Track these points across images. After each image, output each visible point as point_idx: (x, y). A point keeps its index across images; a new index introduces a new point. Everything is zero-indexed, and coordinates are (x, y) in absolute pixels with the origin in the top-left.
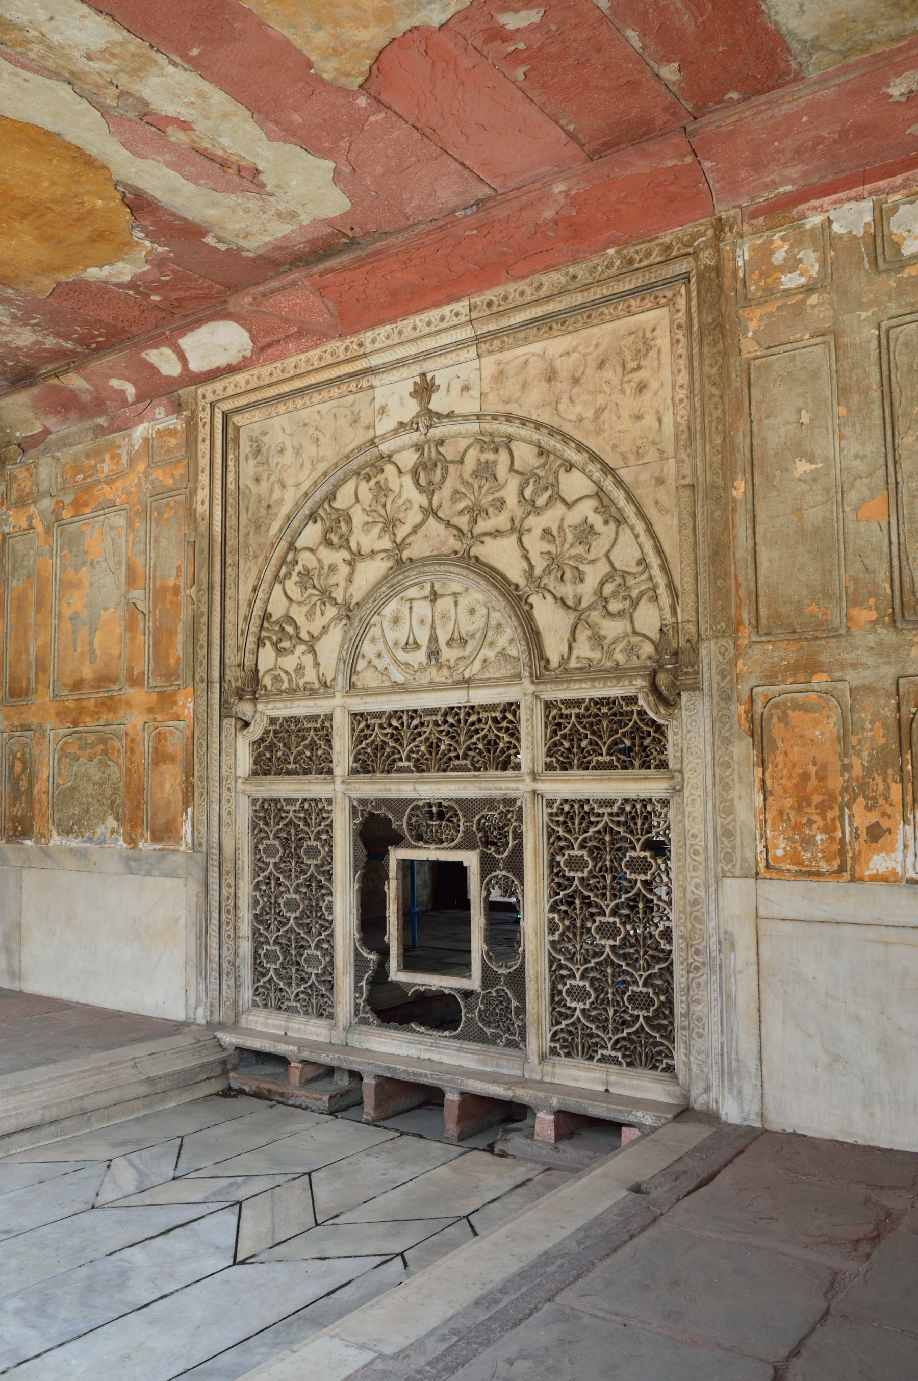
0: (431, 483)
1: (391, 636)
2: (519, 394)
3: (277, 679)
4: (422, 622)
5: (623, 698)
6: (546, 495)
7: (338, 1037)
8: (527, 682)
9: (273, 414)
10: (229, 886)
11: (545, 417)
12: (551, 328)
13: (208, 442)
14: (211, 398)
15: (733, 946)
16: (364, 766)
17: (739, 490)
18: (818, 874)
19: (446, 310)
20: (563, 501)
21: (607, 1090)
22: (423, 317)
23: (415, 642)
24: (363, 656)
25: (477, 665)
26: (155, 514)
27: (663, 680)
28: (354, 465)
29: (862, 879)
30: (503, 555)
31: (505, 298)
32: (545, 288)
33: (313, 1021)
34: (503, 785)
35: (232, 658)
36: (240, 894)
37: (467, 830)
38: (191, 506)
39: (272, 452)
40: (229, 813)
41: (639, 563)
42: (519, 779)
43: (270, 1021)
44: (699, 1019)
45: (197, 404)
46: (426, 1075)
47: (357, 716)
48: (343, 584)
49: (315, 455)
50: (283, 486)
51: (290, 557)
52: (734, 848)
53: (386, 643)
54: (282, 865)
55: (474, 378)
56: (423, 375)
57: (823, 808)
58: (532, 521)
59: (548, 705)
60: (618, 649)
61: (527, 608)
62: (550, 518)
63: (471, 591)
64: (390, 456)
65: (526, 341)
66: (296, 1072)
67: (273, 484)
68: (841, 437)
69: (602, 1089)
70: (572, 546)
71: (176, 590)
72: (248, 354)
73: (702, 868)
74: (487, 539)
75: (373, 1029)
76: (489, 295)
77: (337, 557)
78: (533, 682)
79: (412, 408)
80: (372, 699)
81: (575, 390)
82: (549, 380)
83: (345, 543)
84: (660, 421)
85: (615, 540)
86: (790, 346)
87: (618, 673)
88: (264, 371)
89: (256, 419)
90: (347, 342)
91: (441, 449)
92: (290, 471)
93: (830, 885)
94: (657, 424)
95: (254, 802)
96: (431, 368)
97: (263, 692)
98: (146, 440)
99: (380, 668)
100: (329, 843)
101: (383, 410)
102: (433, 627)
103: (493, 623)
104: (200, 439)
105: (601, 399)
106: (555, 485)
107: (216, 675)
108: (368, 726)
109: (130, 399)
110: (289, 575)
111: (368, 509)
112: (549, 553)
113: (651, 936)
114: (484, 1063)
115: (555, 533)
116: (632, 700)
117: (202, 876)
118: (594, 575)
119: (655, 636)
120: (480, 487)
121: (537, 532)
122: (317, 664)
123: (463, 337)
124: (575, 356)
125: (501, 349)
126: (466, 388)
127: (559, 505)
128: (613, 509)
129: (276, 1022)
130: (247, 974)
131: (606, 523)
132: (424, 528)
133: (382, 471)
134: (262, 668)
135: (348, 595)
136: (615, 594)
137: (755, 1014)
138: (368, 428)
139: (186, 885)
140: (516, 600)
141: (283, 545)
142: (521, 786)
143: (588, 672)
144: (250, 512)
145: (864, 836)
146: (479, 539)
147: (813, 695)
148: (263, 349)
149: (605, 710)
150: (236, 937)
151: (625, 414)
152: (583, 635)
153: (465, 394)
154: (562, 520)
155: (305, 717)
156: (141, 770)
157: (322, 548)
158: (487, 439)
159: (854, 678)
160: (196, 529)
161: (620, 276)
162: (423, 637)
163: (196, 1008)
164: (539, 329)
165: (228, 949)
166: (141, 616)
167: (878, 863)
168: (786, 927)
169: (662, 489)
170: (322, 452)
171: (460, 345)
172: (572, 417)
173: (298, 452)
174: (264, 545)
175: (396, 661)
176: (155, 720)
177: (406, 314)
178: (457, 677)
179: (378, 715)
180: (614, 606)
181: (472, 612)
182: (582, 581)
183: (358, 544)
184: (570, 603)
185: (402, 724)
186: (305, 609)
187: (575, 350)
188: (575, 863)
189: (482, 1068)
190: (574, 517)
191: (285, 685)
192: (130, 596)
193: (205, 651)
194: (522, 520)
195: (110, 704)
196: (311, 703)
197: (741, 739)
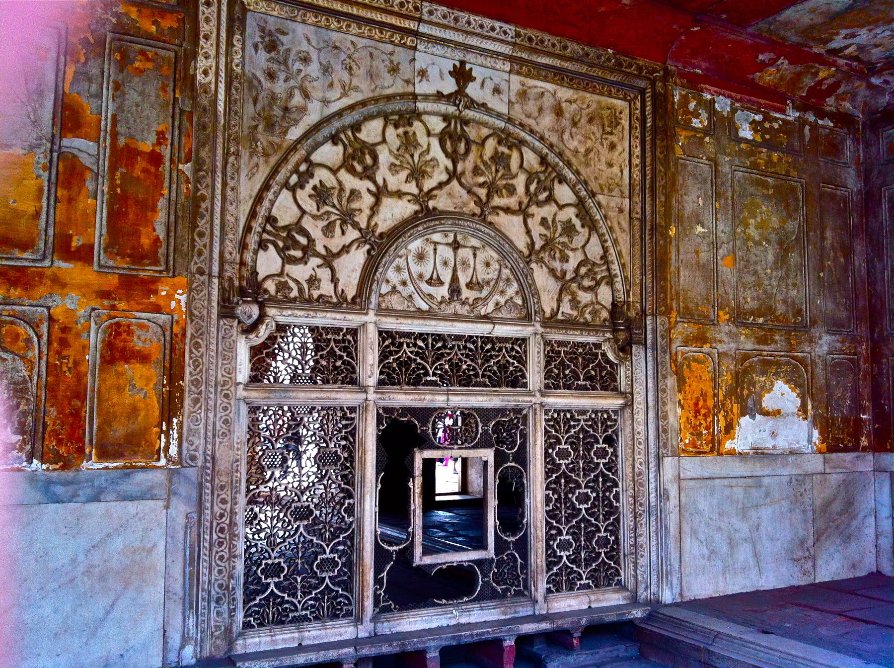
1: (415, 269)
2: (537, 114)
3: (282, 287)
5: (593, 344)
7: (364, 631)
8: (538, 325)
9: (299, 19)
10: (224, 501)
11: (554, 139)
12: (563, 79)
15: (668, 498)
16: (389, 378)
17: (672, 232)
18: (705, 453)
19: (497, 24)
21: (590, 607)
23: (439, 278)
24: (388, 281)
25: (491, 307)
29: (722, 455)
32: (568, 50)
34: (517, 398)
37: (485, 432)
38: (186, 69)
39: (292, 55)
40: (226, 422)
42: (531, 394)
43: (278, 637)
44: (642, 546)
46: (488, 632)
48: (367, 212)
50: (306, 96)
52: (667, 439)
55: (504, 86)
56: (463, 63)
57: (706, 416)
58: (533, 209)
59: (547, 343)
65: (545, 79)
68: (717, 219)
70: (561, 235)
71: (155, 159)
73: (643, 452)
74: (501, 213)
75: (396, 614)
76: (530, 32)
77: (363, 185)
79: (449, 86)
80: (442, 323)
81: (574, 130)
84: (622, 171)
85: (589, 239)
86: (696, 160)
87: (586, 327)
89: (275, 13)
91: (465, 128)
92: (315, 83)
93: (710, 458)
94: (620, 174)
96: (472, 61)
99: (405, 294)
101: (423, 73)
102: (455, 270)
103: (504, 277)
105: (589, 144)
106: (551, 190)
107: (216, 269)
108: (393, 344)
110: (301, 185)
112: (545, 235)
113: (608, 498)
114: (505, 613)
116: (598, 346)
117: (195, 495)
118: (574, 259)
120: (497, 171)
121: (538, 219)
122: (334, 280)
123: (502, 51)
124: (574, 106)
125: (527, 76)
127: (553, 204)
129: (285, 636)
130: (240, 595)
131: (583, 226)
132: (448, 187)
133: (411, 125)
134: (262, 272)
135: (373, 223)
136: (586, 275)
137: (678, 535)
138: (408, 82)
139: (167, 507)
141: (302, 152)
142: (534, 400)
143: (569, 324)
144: (259, 106)
145: (723, 431)
146: (496, 209)
147: (701, 355)
149: (580, 350)
151: (603, 160)
152: (566, 298)
153: (496, 94)
154: (555, 215)
155: (323, 328)
156: (82, 368)
158: (503, 136)
159: (722, 348)
160: (194, 98)
161: (612, 71)
162: (446, 277)
163: (183, 646)
164: (555, 76)
165: (220, 572)
167: (728, 445)
168: (692, 483)
169: (622, 217)
170: (355, 82)
171: (496, 55)
172: (572, 148)
173: (326, 70)
174: (280, 146)
176: (113, 307)
179: (408, 335)
180: (587, 283)
181: (488, 265)
182: (567, 261)
183: (384, 180)
184: (559, 274)
185: (427, 345)
186: (322, 224)
187: (575, 101)
188: (563, 454)
189: (503, 617)
190: (563, 215)
191: (294, 293)
192: (66, 142)
196: (339, 316)
197: (671, 376)
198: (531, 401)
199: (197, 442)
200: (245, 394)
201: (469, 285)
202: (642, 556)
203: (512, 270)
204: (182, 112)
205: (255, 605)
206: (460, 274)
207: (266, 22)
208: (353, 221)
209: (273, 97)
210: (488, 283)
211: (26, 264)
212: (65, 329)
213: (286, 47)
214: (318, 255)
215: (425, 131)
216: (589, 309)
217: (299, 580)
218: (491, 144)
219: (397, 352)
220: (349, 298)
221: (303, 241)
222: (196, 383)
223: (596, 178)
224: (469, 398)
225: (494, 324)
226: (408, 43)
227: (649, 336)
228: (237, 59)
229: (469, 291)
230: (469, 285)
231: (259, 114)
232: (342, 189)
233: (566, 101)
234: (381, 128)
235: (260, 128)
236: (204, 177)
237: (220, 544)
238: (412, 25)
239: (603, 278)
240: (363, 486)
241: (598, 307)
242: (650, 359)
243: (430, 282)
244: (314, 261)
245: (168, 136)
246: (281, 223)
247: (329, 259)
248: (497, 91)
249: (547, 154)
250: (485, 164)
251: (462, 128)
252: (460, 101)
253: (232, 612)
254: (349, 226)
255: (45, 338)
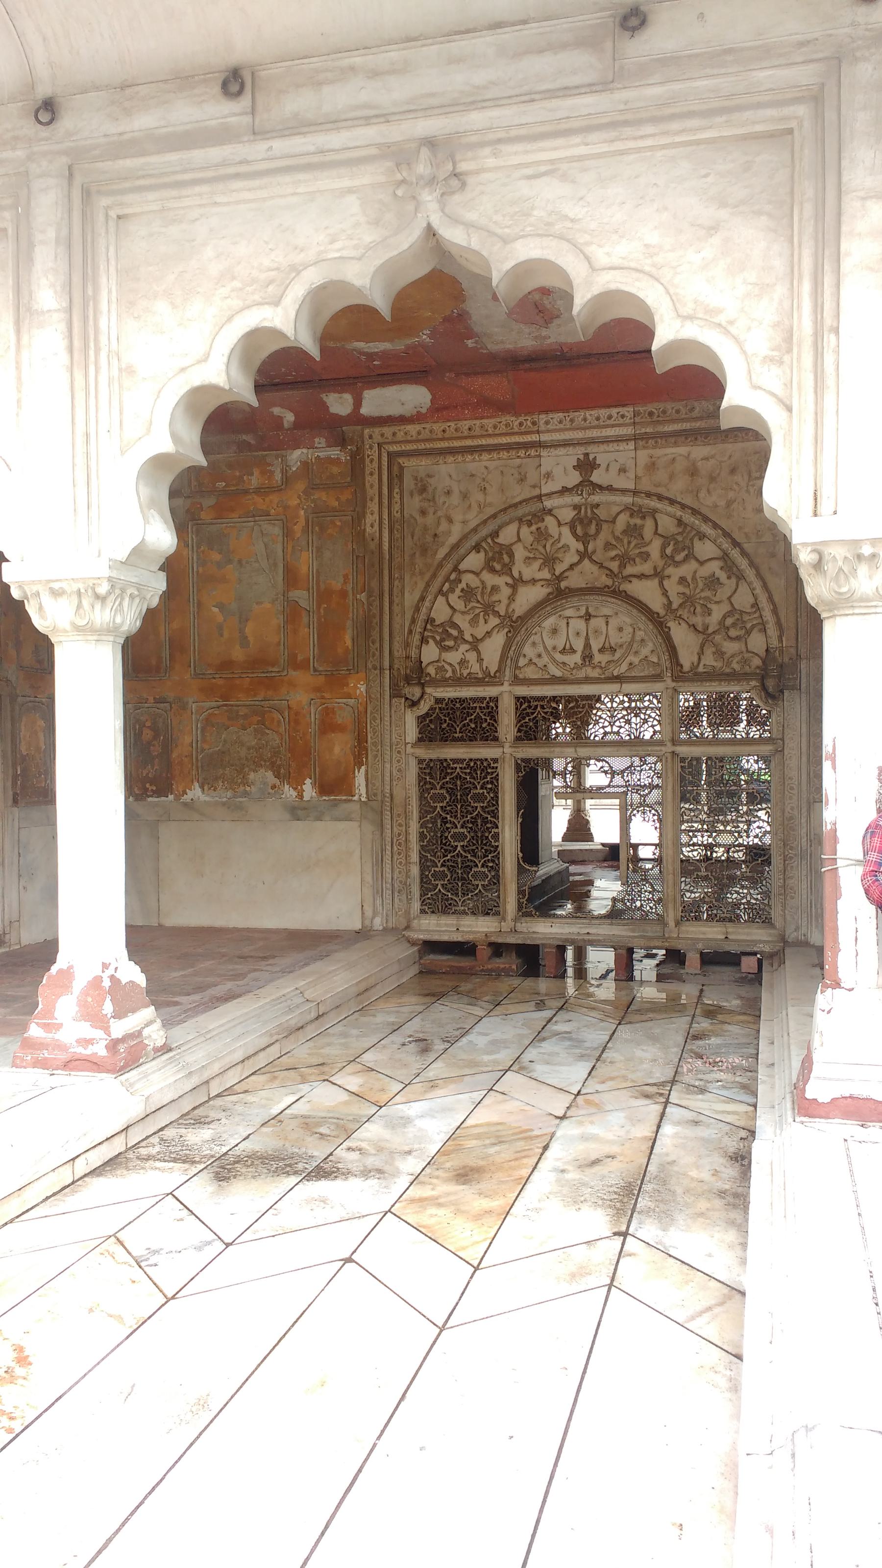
0: (586, 534)
1: (549, 643)
4: (578, 633)
6: (683, 554)
10: (400, 825)
11: (688, 501)
12: (696, 439)
13: (376, 476)
14: (377, 438)
19: (614, 411)
20: (697, 560)
22: (593, 412)
23: (571, 648)
24: (525, 656)
25: (624, 667)
26: (317, 528)
27: (770, 684)
28: (520, 512)
30: (647, 592)
31: (664, 412)
32: (697, 411)
33: (481, 918)
35: (399, 652)
36: (411, 830)
40: (399, 770)
41: (753, 606)
45: (363, 442)
47: (520, 700)
48: (505, 601)
49: (482, 500)
50: (450, 521)
51: (453, 577)
53: (545, 647)
54: (448, 808)
55: (630, 464)
56: (586, 455)
58: (670, 570)
60: (735, 661)
61: (667, 630)
62: (686, 570)
63: (620, 615)
64: (550, 510)
65: (676, 444)
66: (483, 952)
67: (439, 518)
69: (723, 937)
70: (702, 590)
71: (343, 594)
72: (424, 411)
74: (634, 580)
76: (651, 407)
77: (501, 581)
78: (673, 681)
79: (575, 478)
81: (712, 486)
82: (692, 475)
83: (507, 569)
88: (438, 427)
89: (423, 463)
90: (521, 419)
95: (421, 761)
97: (428, 679)
98: (305, 464)
99: (540, 665)
100: (495, 791)
101: (548, 475)
102: (587, 638)
103: (638, 638)
104: (367, 472)
105: (731, 495)
106: (691, 548)
107: (386, 664)
108: (530, 707)
109: (286, 425)
110: (452, 590)
111: (530, 547)
112: (683, 594)
114: (633, 931)
115: (689, 580)
119: (763, 653)
120: (629, 543)
122: (480, 660)
124: (712, 462)
125: (654, 447)
126: (623, 470)
128: (735, 569)
131: (729, 578)
132: (580, 566)
133: (543, 520)
134: (425, 660)
136: (734, 625)
138: (534, 487)
139: (360, 826)
140: (659, 623)
141: (449, 566)
142: (663, 748)
146: (628, 578)
148: (438, 410)
150: (408, 863)
152: (709, 651)
154: (695, 572)
155: (471, 699)
157: (484, 572)
162: (579, 645)
163: (373, 918)
165: (400, 872)
166: (304, 614)
170: (489, 499)
173: (465, 496)
175: (554, 660)
176: (323, 698)
177: (577, 409)
178: (608, 674)
180: (733, 633)
181: (620, 629)
182: (709, 614)
186: (468, 617)
187: (713, 457)
191: (449, 674)
192: (291, 594)
193: (378, 645)
194: (663, 569)
195: (271, 684)
198: (661, 750)
199: (377, 784)
200: (412, 750)
201: (601, 650)
202: (792, 898)
203: (645, 631)
204: (357, 557)
205: (428, 898)
206: (592, 642)
207: (418, 472)
208: (493, 610)
209: (425, 528)
210: (621, 646)
211: (273, 674)
212: (297, 714)
213: (433, 487)
214: (466, 642)
215: (556, 523)
216: (736, 659)
217: (460, 884)
218: (623, 519)
219: (533, 713)
220: (492, 675)
221: (455, 633)
222: (374, 744)
223: (740, 528)
224: (596, 749)
225: (621, 683)
226: (532, 454)
227: (804, 681)
228: (397, 507)
229: (601, 655)
230: (601, 650)
231: (416, 544)
232: (484, 587)
233: (702, 459)
234: (516, 530)
235: (417, 555)
236: (374, 601)
237: (399, 854)
238: (534, 438)
239: (753, 626)
240: (503, 820)
241: (746, 655)
242: (804, 704)
243: (563, 651)
244: (464, 647)
245: (351, 577)
246: (437, 623)
247: (475, 644)
248: (623, 470)
249: (681, 516)
250: (617, 539)
251: (593, 512)
252: (582, 491)
253: (409, 900)
254: (491, 616)
255: (287, 720)
